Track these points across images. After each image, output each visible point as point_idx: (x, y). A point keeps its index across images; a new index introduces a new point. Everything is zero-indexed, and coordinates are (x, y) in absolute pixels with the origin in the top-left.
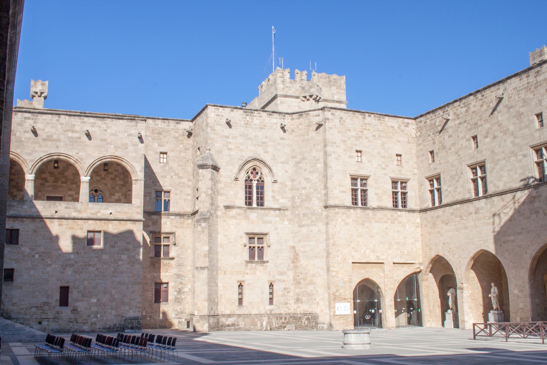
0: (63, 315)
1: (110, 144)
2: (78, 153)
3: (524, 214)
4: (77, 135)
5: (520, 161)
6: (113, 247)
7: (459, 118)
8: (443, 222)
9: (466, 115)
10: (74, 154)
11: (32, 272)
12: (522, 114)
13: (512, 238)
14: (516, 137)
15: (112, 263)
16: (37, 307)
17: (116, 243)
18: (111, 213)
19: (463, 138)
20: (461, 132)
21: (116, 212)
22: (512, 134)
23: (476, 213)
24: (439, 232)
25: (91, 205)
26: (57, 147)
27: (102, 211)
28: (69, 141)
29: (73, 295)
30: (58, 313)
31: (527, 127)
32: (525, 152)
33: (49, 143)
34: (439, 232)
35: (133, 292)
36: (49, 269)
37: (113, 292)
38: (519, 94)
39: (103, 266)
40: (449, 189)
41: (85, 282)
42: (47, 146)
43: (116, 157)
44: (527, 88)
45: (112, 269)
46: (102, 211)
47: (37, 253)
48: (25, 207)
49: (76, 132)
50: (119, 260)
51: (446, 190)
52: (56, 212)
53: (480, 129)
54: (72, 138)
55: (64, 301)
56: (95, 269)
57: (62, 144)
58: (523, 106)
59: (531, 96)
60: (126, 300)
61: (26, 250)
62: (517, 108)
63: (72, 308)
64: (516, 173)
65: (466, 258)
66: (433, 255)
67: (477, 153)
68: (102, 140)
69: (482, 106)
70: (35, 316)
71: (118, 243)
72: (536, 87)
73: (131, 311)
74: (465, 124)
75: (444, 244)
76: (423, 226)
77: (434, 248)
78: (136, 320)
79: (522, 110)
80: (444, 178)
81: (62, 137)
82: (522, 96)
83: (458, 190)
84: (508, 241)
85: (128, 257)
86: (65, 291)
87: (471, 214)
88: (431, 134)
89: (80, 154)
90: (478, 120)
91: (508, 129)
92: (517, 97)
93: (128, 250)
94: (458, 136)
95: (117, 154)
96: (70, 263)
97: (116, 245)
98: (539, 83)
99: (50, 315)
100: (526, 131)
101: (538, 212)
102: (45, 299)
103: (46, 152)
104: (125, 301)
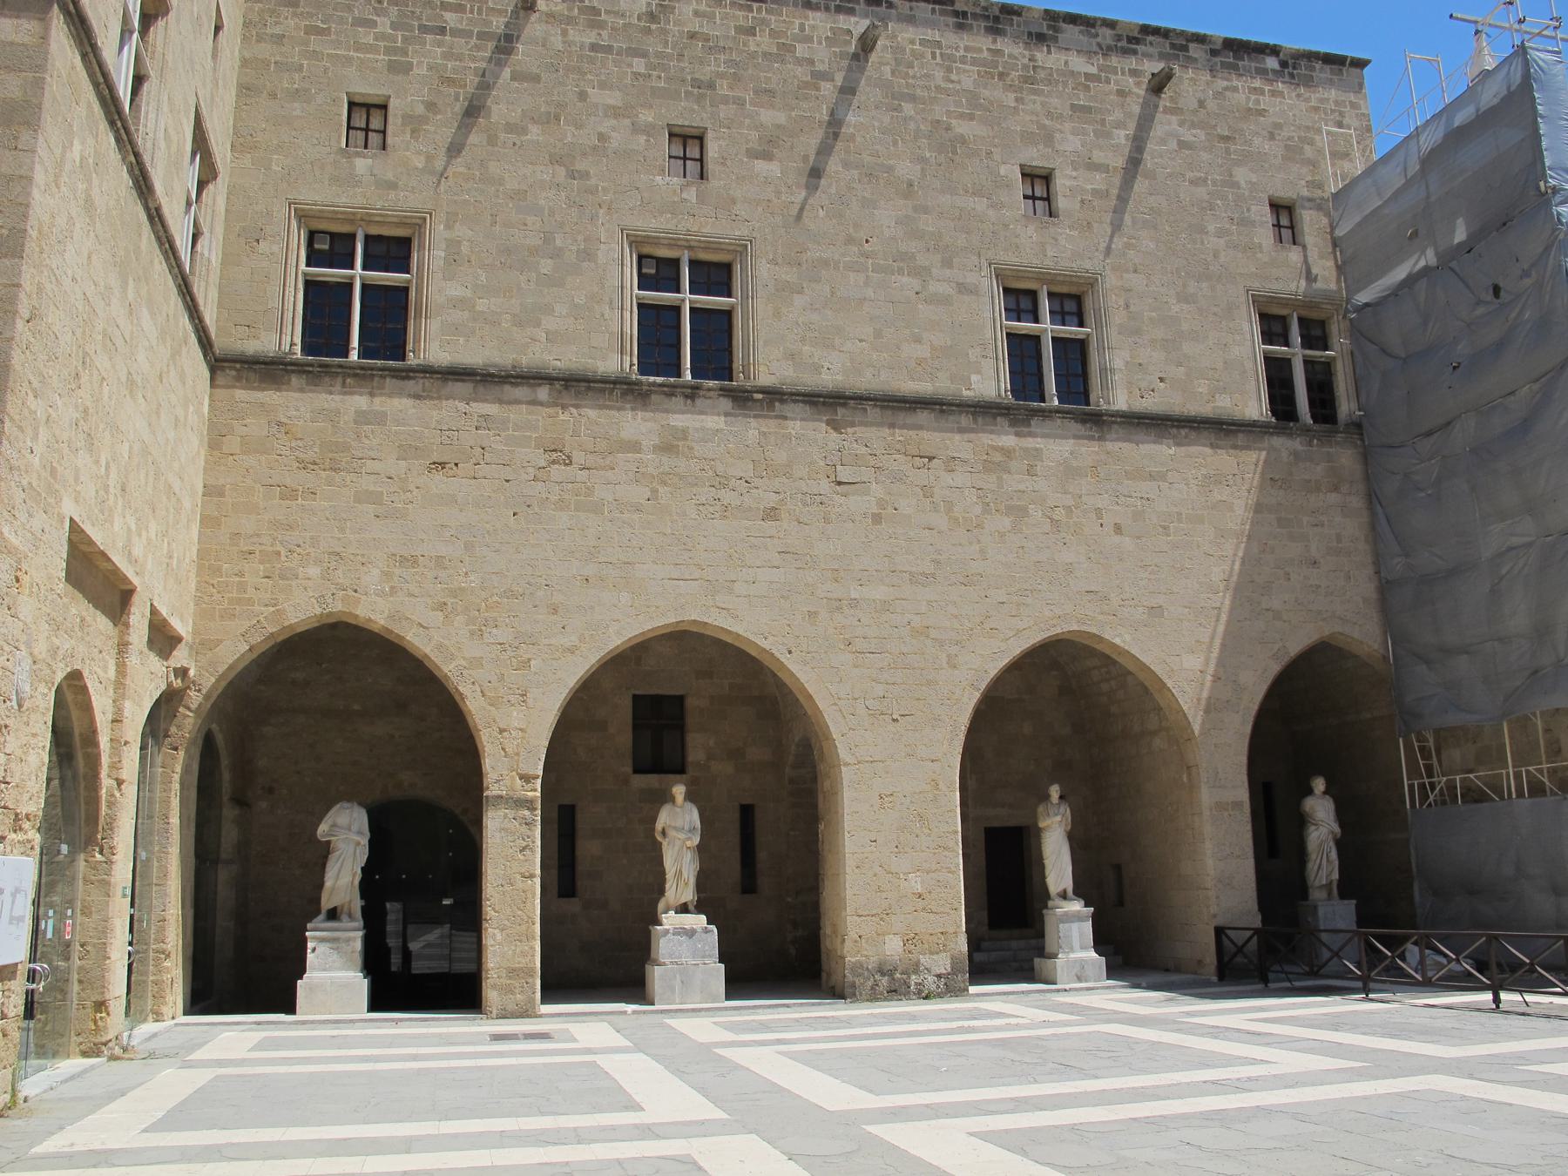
3: (950, 506)
5: (944, 301)
7: (596, 25)
8: (407, 451)
9: (648, 31)
12: (963, 140)
13: (879, 592)
14: (925, 210)
19: (615, 112)
20: (603, 86)
22: (908, 190)
23: (667, 448)
24: (374, 498)
31: (977, 193)
32: (971, 278)
34: (374, 498)
38: (949, 70)
40: (482, 305)
44: (994, 71)
51: (458, 303)
53: (724, 111)
58: (971, 117)
59: (1010, 99)
62: (938, 112)
64: (918, 340)
65: (572, 650)
66: (301, 608)
67: (701, 199)
69: (751, 31)
72: (1026, 80)
74: (639, 65)
75: (411, 561)
76: (232, 444)
77: (314, 571)
79: (961, 128)
80: (453, 245)
82: (968, 83)
83: (549, 323)
84: (854, 603)
87: (635, 447)
88: (384, 25)
90: (722, 76)
91: (890, 169)
92: (939, 74)
94: (583, 96)
98: (1042, 74)
100: (980, 205)
101: (1019, 512)
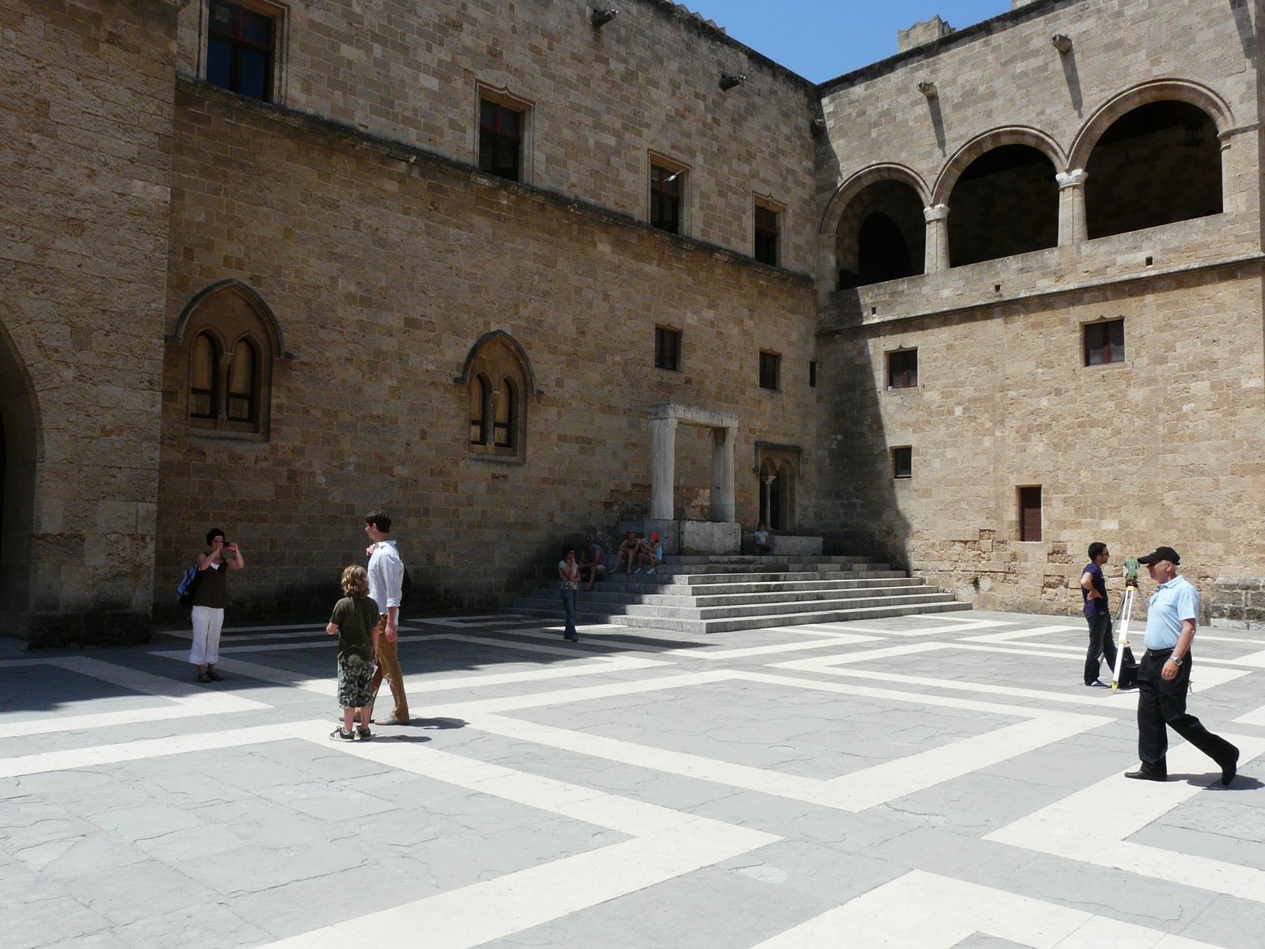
0: (1028, 564)
1: (1134, 49)
2: (1043, 112)
4: (1036, 62)
6: (1161, 360)
10: (1034, 115)
11: (950, 453)
15: (1159, 410)
16: (966, 542)
17: (1171, 348)
18: (1149, 261)
21: (1166, 251)
25: (1088, 248)
26: (989, 114)
27: (1121, 260)
28: (1019, 87)
29: (1050, 512)
30: (1014, 557)
33: (970, 111)
35: (1238, 499)
36: (987, 441)
37: (1168, 499)
39: (1131, 421)
41: (1083, 473)
42: (964, 120)
43: (1160, 85)
45: (1162, 430)
46: (1121, 260)
47: (959, 404)
48: (926, 290)
49: (1035, 53)
50: (1187, 400)
52: (998, 288)
54: (1024, 74)
55: (1029, 528)
56: (1108, 432)
57: (997, 103)
60: (1212, 524)
61: (932, 396)
63: (1049, 547)
68: (1108, 48)
70: (962, 565)
71: (1178, 345)
73: (1232, 559)
78: (1247, 588)
81: (998, 84)
85: (1213, 387)
86: (1030, 498)
89: (1048, 111)
93: (1213, 363)
95: (1158, 72)
96: (1039, 421)
97: (1171, 355)
99: (996, 562)
102: (982, 523)
103: (962, 136)
104: (1209, 527)
